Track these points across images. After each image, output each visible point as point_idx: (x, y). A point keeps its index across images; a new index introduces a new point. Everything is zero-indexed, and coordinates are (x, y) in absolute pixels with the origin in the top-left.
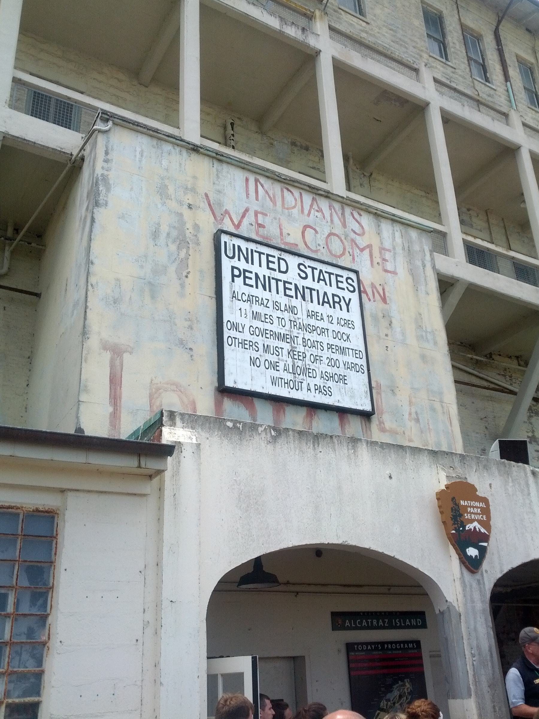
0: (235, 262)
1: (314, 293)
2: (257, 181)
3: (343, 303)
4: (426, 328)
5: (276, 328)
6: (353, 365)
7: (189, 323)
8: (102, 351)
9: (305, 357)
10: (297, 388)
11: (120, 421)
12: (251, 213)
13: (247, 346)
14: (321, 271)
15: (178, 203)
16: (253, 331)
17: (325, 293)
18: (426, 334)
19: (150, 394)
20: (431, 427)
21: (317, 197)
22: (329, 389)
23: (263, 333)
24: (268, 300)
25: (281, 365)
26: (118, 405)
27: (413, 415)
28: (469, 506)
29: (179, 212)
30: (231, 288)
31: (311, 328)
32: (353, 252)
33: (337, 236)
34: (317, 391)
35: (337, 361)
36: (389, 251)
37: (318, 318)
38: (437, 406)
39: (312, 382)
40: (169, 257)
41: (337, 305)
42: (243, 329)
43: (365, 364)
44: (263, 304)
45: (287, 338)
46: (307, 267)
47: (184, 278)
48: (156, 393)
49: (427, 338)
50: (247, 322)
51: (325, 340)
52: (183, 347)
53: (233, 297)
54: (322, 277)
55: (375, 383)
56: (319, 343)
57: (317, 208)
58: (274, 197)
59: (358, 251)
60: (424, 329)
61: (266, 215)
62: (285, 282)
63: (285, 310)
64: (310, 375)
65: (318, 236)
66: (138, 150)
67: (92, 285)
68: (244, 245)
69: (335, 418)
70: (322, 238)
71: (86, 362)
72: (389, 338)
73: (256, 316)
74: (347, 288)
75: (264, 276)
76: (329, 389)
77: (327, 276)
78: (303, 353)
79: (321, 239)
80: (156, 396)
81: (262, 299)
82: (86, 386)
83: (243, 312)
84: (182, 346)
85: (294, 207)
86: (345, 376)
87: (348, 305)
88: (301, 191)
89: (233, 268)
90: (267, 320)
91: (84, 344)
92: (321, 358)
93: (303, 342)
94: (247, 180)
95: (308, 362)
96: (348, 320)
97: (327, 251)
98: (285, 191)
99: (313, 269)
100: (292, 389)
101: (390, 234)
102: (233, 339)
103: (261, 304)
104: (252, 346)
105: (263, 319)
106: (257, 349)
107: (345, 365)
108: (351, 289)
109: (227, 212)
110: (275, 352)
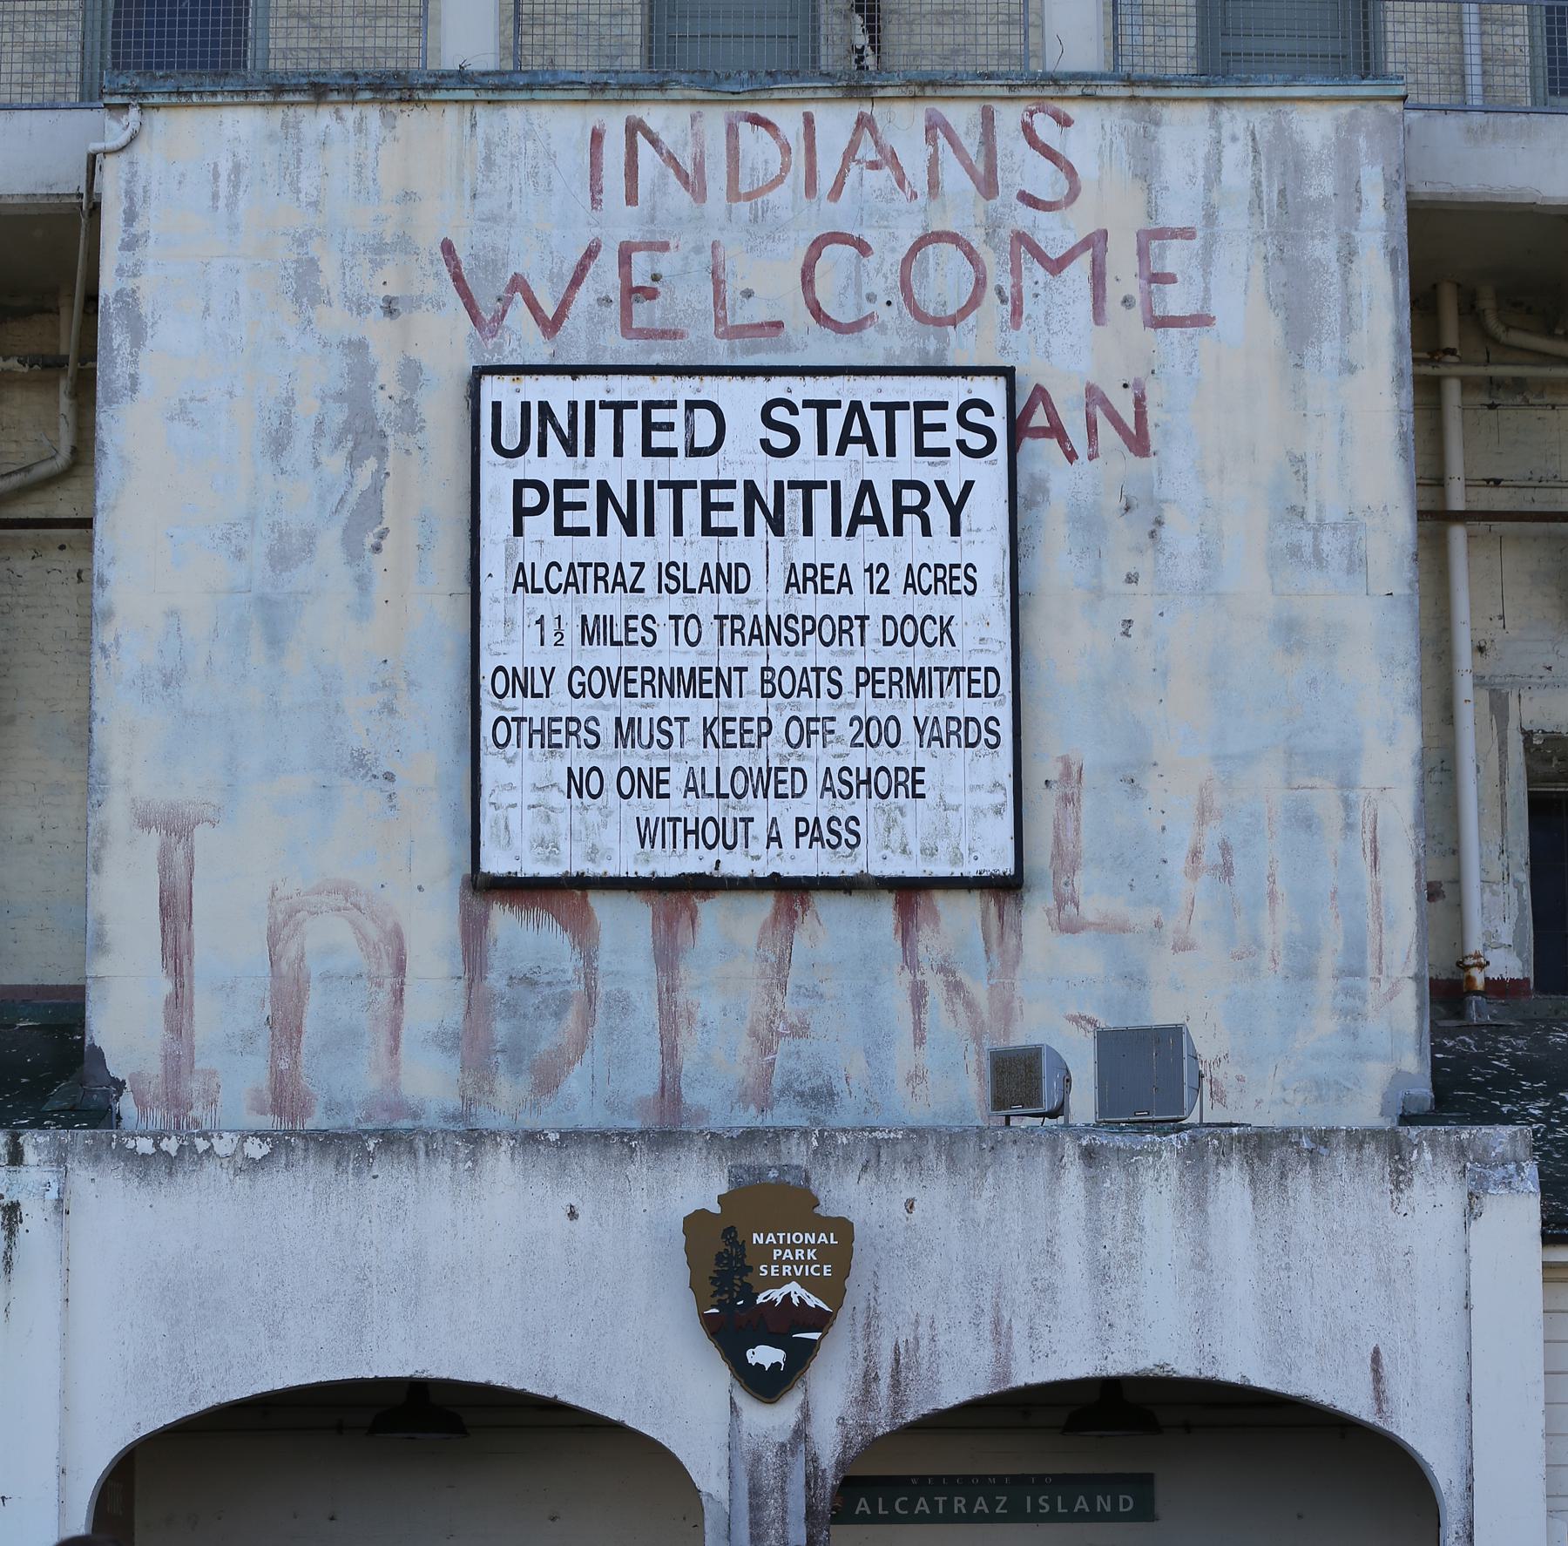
0: (530, 466)
1: (822, 499)
2: (634, 128)
3: (937, 512)
4: (1320, 509)
5: (670, 655)
6: (954, 726)
7: (382, 696)
8: (138, 831)
9: (768, 734)
10: (730, 842)
11: (191, 1016)
12: (608, 260)
13: (556, 739)
14: (856, 407)
15: (350, 309)
16: (580, 684)
17: (867, 487)
18: (1315, 538)
19: (270, 929)
20: (1280, 888)
21: (878, 111)
22: (852, 825)
23: (619, 681)
24: (642, 565)
25: (677, 778)
26: (185, 973)
27: (1211, 856)
28: (778, 1246)
29: (354, 337)
30: (509, 557)
31: (799, 628)
32: (1017, 287)
33: (954, 238)
34: (805, 841)
35: (892, 722)
36: (1187, 234)
37: (828, 585)
38: (1326, 802)
39: (786, 813)
40: (322, 498)
41: (911, 522)
42: (548, 683)
43: (1005, 714)
44: (623, 584)
45: (703, 682)
46: (799, 405)
47: (368, 554)
48: (286, 924)
49: (1317, 554)
50: (573, 654)
51: (848, 660)
52: (364, 777)
53: (517, 584)
54: (856, 431)
55: (1060, 766)
56: (824, 675)
57: (872, 155)
58: (699, 166)
59: (1040, 273)
60: (1311, 517)
61: (664, 247)
62: (708, 486)
63: (703, 584)
64: (782, 789)
65: (871, 262)
66: (225, 167)
67: (103, 648)
68: (559, 393)
69: (885, 910)
70: (886, 268)
71: (97, 870)
72: (1144, 584)
73: (596, 629)
74: (961, 444)
75: (632, 485)
76: (852, 825)
77: (877, 420)
78: (760, 719)
79: (881, 274)
80: (285, 932)
81: (620, 566)
82: (100, 935)
83: (550, 626)
84: (363, 772)
85: (779, 180)
86: (915, 770)
87: (955, 510)
88: (810, 108)
89: (519, 486)
90: (632, 637)
91: (90, 821)
92: (830, 725)
93: (763, 681)
94: (597, 137)
95: (775, 746)
96: (953, 566)
97: (906, 311)
98: (745, 128)
99: (822, 407)
100: (710, 847)
101: (1201, 164)
102: (514, 725)
103: (616, 584)
104: (575, 734)
105: (619, 634)
106: (592, 740)
107: (921, 732)
108: (976, 441)
109: (519, 284)
110: (657, 735)
